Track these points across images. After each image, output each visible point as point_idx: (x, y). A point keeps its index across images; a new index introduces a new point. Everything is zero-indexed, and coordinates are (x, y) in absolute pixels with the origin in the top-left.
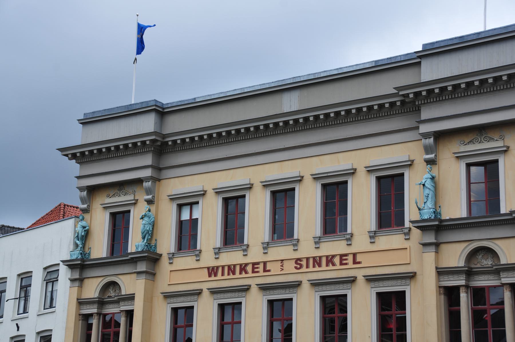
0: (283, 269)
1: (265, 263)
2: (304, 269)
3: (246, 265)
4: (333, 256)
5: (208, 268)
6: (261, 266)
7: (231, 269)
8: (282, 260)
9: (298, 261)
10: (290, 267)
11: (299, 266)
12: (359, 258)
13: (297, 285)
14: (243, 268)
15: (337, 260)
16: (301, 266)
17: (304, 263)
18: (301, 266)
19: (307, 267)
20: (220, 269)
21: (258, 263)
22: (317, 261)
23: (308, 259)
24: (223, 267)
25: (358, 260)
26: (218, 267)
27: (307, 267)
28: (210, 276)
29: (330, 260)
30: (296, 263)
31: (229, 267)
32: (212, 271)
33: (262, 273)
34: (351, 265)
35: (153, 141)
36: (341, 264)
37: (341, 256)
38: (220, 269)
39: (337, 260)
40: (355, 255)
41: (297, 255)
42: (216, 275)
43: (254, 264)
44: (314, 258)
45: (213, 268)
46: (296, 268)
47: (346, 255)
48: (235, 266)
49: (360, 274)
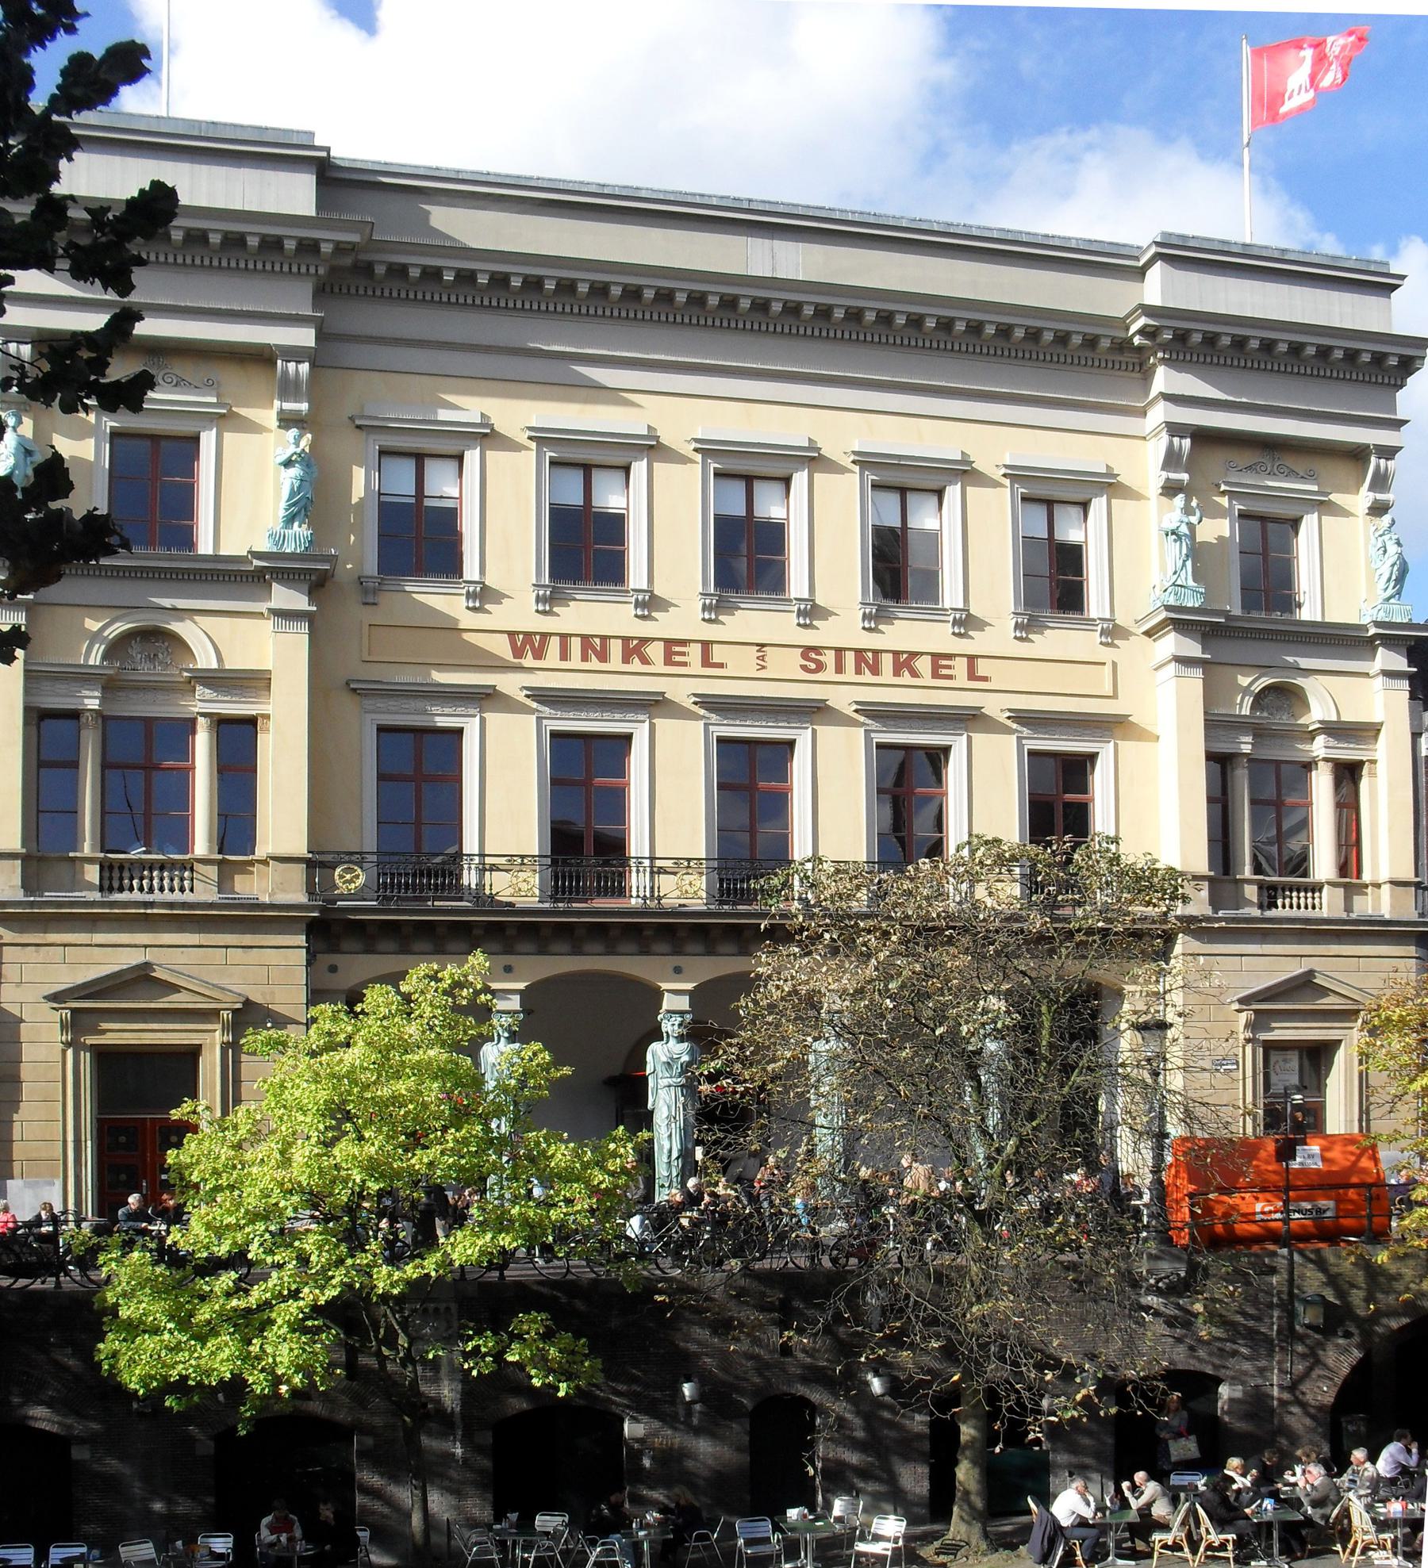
0: (763, 667)
1: (706, 645)
2: (829, 674)
3: (645, 641)
4: (914, 655)
5: (512, 634)
6: (695, 651)
7: (595, 647)
8: (763, 645)
9: (808, 651)
10: (789, 664)
11: (813, 666)
12: (983, 667)
13: (813, 711)
14: (634, 648)
15: (924, 665)
16: (820, 667)
17: (829, 658)
18: (820, 667)
19: (839, 669)
20: (554, 644)
21: (683, 642)
22: (868, 660)
23: (839, 651)
24: (564, 638)
25: (980, 673)
26: (545, 636)
27: (839, 669)
28: (518, 652)
29: (904, 662)
30: (804, 656)
31: (585, 639)
32: (528, 643)
33: (696, 667)
34: (962, 680)
35: (340, 248)
36: (935, 675)
37: (936, 657)
38: (554, 644)
39: (924, 665)
40: (972, 659)
41: (809, 638)
42: (539, 654)
43: (669, 643)
44: (859, 652)
45: (528, 635)
46: (804, 668)
47: (949, 657)
48: (604, 639)
49: (995, 707)
